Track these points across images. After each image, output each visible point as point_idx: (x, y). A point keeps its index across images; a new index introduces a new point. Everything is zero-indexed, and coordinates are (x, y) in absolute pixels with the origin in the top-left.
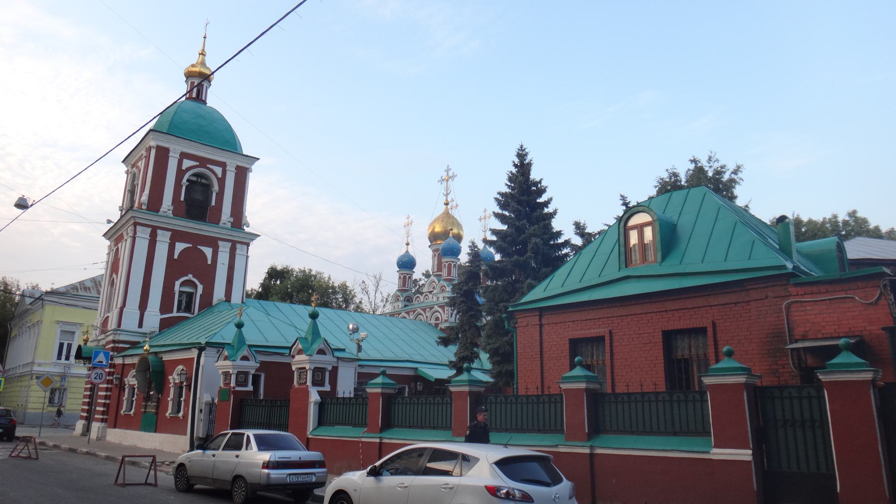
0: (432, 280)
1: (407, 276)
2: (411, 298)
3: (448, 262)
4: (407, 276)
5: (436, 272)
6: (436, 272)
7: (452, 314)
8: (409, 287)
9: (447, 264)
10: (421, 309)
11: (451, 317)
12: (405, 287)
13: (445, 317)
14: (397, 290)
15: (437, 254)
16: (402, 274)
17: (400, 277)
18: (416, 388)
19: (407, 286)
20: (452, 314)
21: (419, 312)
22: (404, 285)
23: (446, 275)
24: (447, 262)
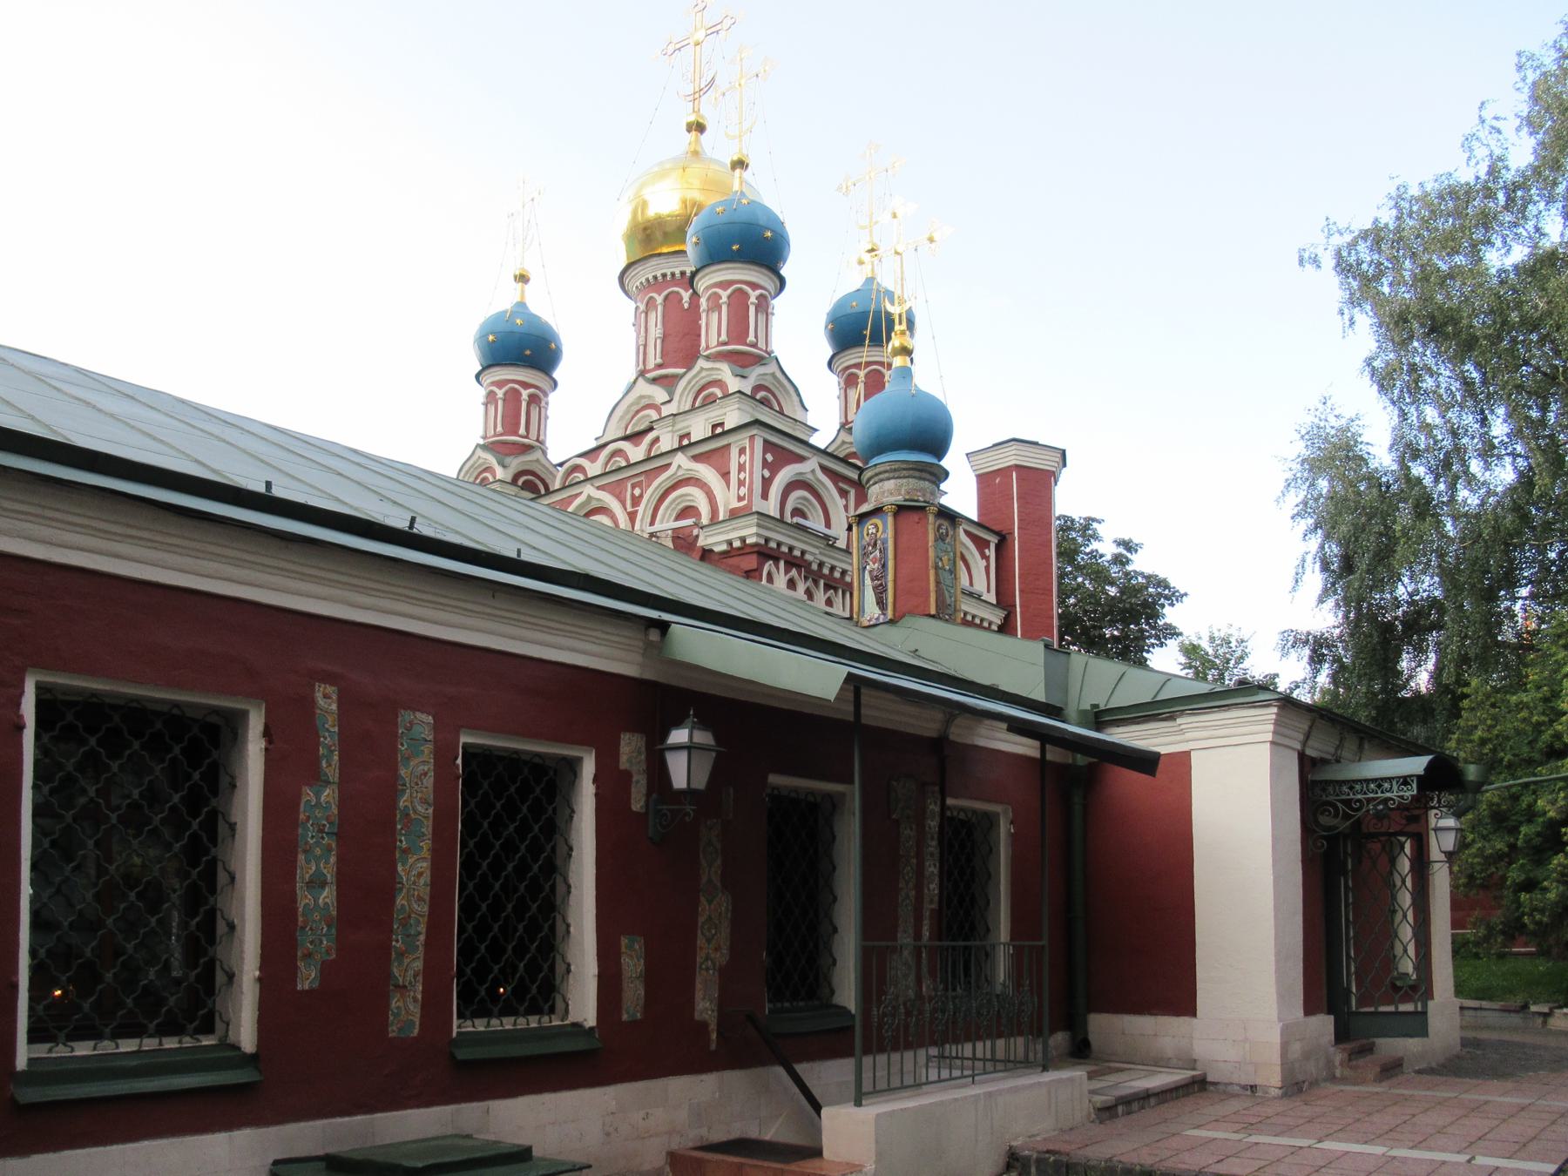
0: (642, 397)
1: (525, 394)
2: (543, 481)
3: (731, 283)
4: (525, 394)
5: (659, 366)
6: (659, 366)
7: (766, 483)
8: (533, 434)
9: (724, 295)
10: (598, 488)
11: (765, 496)
12: (516, 433)
13: (727, 498)
14: (478, 445)
15: (659, 299)
16: (500, 384)
17: (491, 397)
18: (658, 771)
19: (522, 431)
20: (766, 483)
21: (589, 497)
22: (511, 424)
23: (724, 337)
24: (724, 285)
